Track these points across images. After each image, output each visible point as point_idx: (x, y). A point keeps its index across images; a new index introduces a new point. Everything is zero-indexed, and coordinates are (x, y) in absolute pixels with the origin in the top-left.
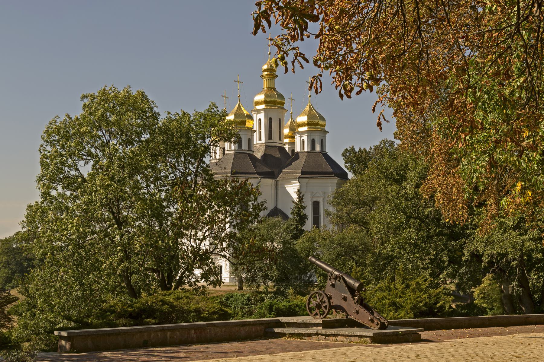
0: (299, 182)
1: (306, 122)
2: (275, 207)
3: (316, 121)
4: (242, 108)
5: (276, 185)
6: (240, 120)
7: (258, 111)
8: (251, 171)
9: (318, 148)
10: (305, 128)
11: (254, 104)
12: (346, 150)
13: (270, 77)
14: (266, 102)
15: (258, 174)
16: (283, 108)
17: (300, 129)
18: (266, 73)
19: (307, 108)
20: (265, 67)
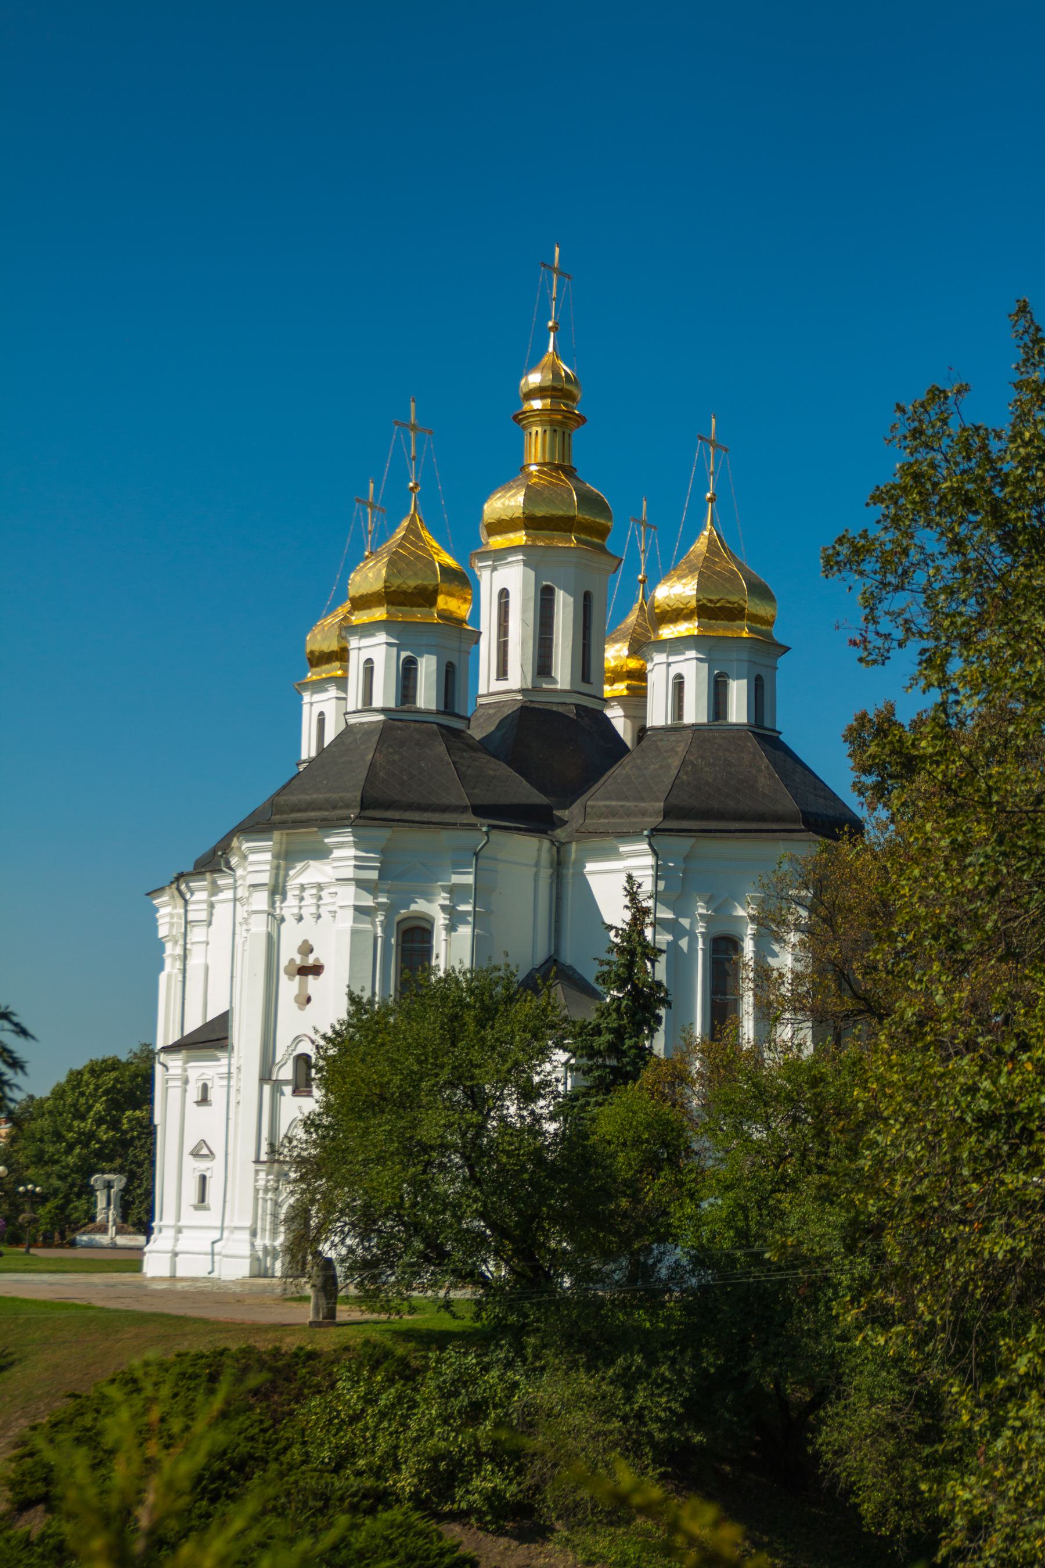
0: (655, 853)
1: (693, 604)
2: (551, 957)
3: (734, 598)
4: (425, 534)
5: (559, 865)
6: (412, 583)
7: (499, 556)
8: (452, 800)
9: (738, 711)
10: (687, 628)
11: (483, 533)
12: (863, 718)
13: (552, 423)
14: (530, 522)
15: (480, 810)
16: (602, 549)
17: (668, 632)
18: (537, 404)
19: (701, 545)
20: (534, 379)
